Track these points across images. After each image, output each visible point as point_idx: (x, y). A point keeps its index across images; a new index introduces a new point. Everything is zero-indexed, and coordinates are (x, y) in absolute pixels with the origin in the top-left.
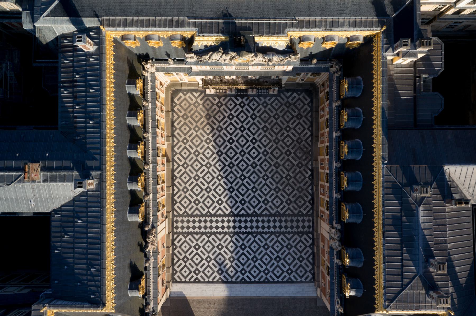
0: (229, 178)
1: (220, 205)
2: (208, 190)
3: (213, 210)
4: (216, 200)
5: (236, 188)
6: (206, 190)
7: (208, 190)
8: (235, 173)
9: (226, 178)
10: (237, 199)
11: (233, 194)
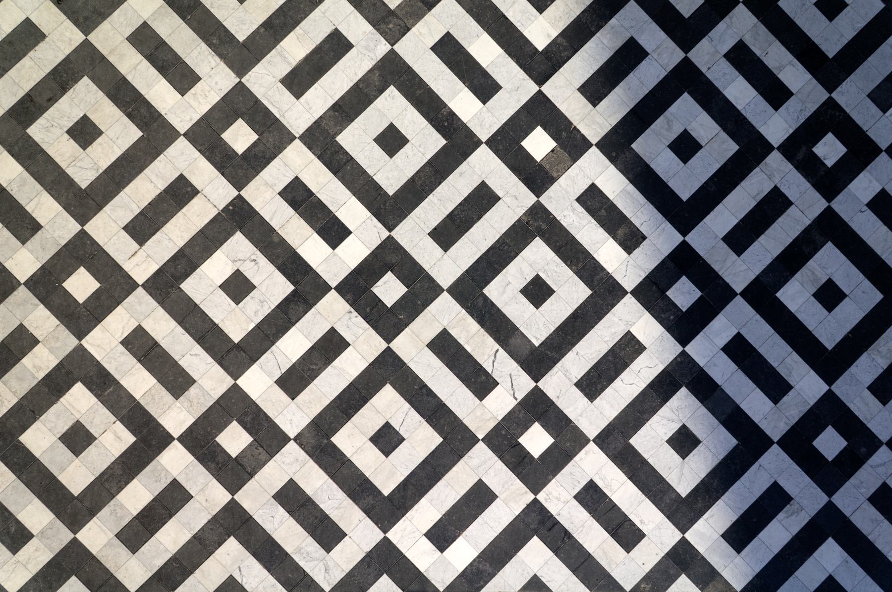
0: (653, 146)
1: (534, 472)
2: (386, 288)
3: (442, 535)
4: (481, 414)
5: (739, 270)
6: (357, 288)
7: (386, 288)
8: (740, 92)
9: (618, 145)
10: (754, 403)
11: (706, 349)
